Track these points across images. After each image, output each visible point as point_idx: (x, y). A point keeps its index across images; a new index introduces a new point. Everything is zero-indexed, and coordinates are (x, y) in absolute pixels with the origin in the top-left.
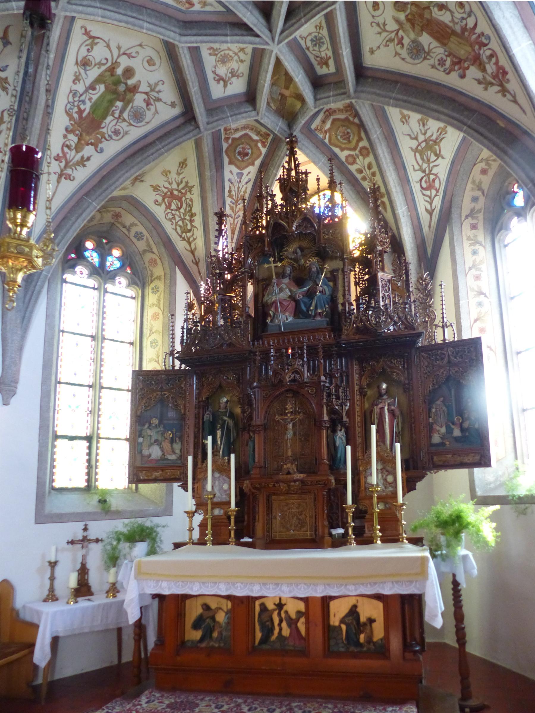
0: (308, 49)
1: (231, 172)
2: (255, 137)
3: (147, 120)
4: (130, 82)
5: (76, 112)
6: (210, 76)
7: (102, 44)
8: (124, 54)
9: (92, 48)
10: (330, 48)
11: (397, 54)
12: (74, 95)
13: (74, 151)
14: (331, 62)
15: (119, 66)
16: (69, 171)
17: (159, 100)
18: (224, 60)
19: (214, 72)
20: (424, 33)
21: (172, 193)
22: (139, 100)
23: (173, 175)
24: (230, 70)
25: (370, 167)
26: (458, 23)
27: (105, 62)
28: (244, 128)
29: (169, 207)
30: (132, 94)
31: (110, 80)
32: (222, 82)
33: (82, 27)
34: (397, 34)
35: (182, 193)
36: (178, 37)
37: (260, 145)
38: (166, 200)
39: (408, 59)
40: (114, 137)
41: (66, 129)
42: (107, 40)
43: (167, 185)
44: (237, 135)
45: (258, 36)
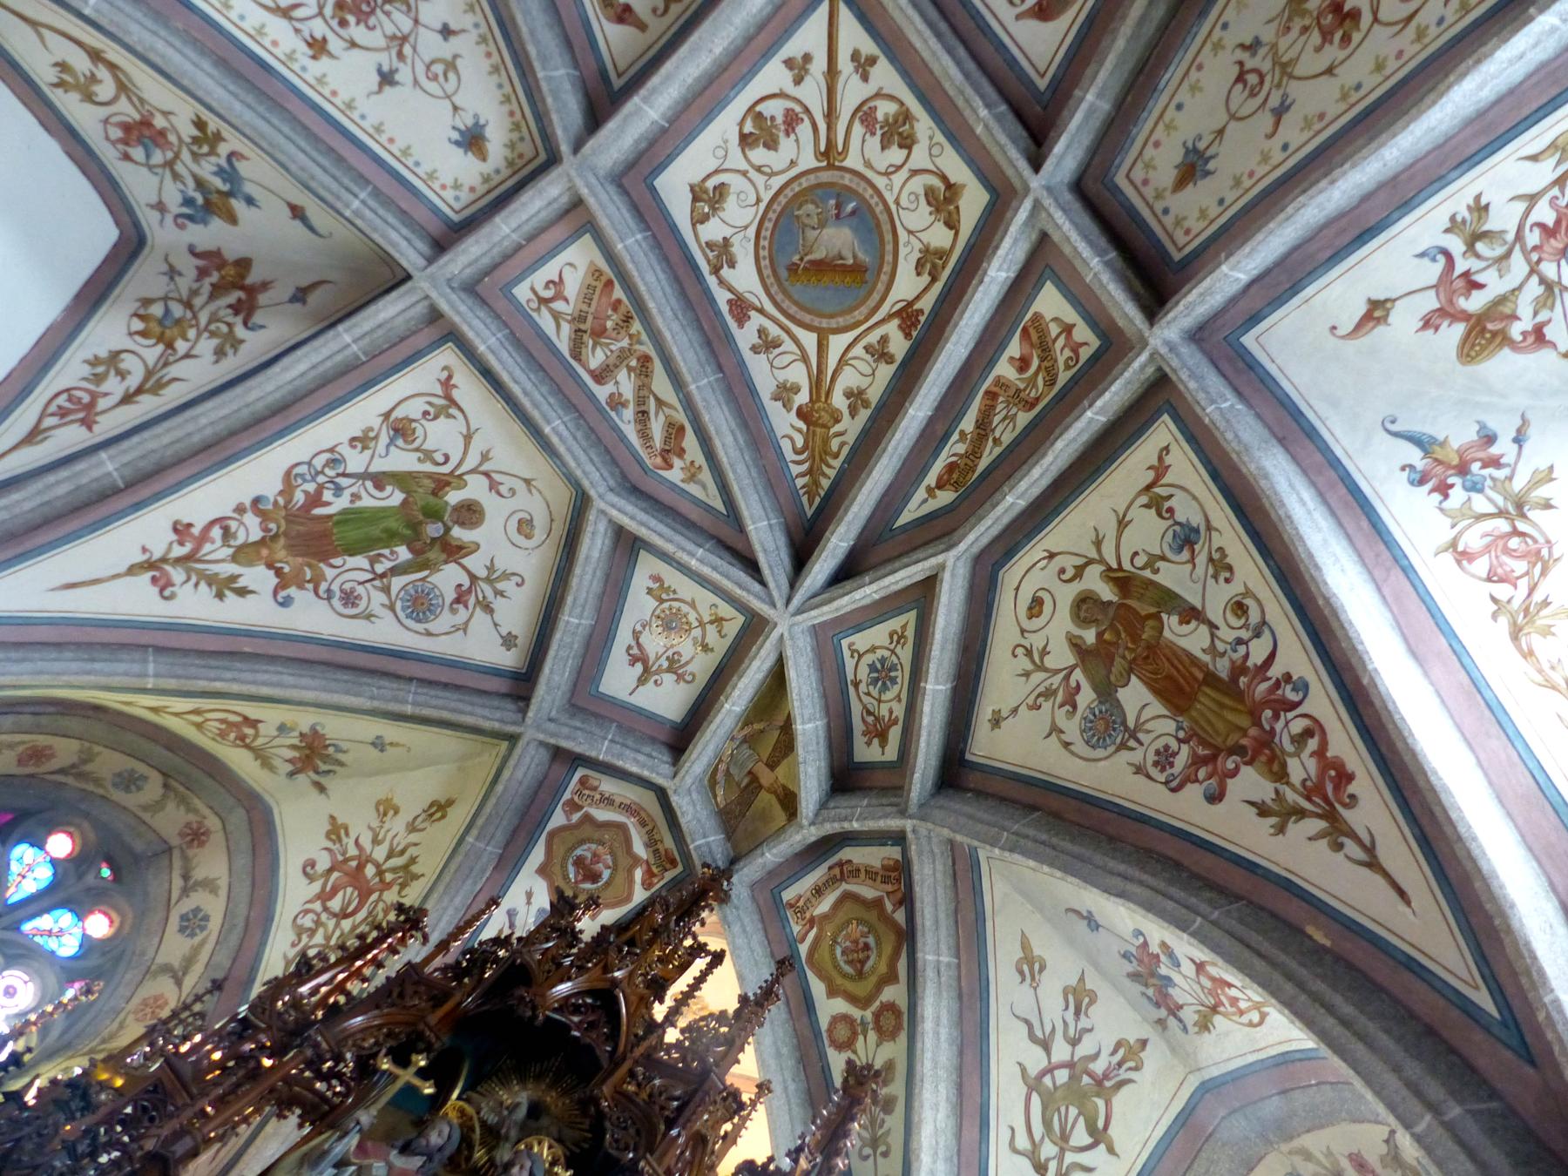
0: (856, 684)
1: (529, 895)
2: (639, 849)
3: (431, 626)
4: (457, 532)
5: (305, 492)
6: (623, 637)
7: (458, 425)
8: (487, 474)
9: (436, 418)
10: (904, 696)
11: (1055, 730)
12: (332, 463)
13: (230, 551)
14: (895, 734)
15: (459, 488)
16: (177, 575)
17: (488, 608)
18: (671, 622)
19: (636, 635)
20: (1133, 678)
21: (360, 868)
22: (448, 578)
23: (397, 825)
24: (670, 653)
26: (1223, 654)
27: (441, 459)
28: (628, 809)
29: (324, 896)
30: (444, 556)
31: (422, 496)
32: (639, 667)
33: (445, 368)
34: (1067, 677)
35: (382, 881)
36: (602, 489)
37: (638, 874)
38: (336, 875)
39: (1080, 747)
40: (336, 602)
41: (256, 501)
42: (473, 428)
43: (366, 841)
44: (602, 815)
45: (763, 583)
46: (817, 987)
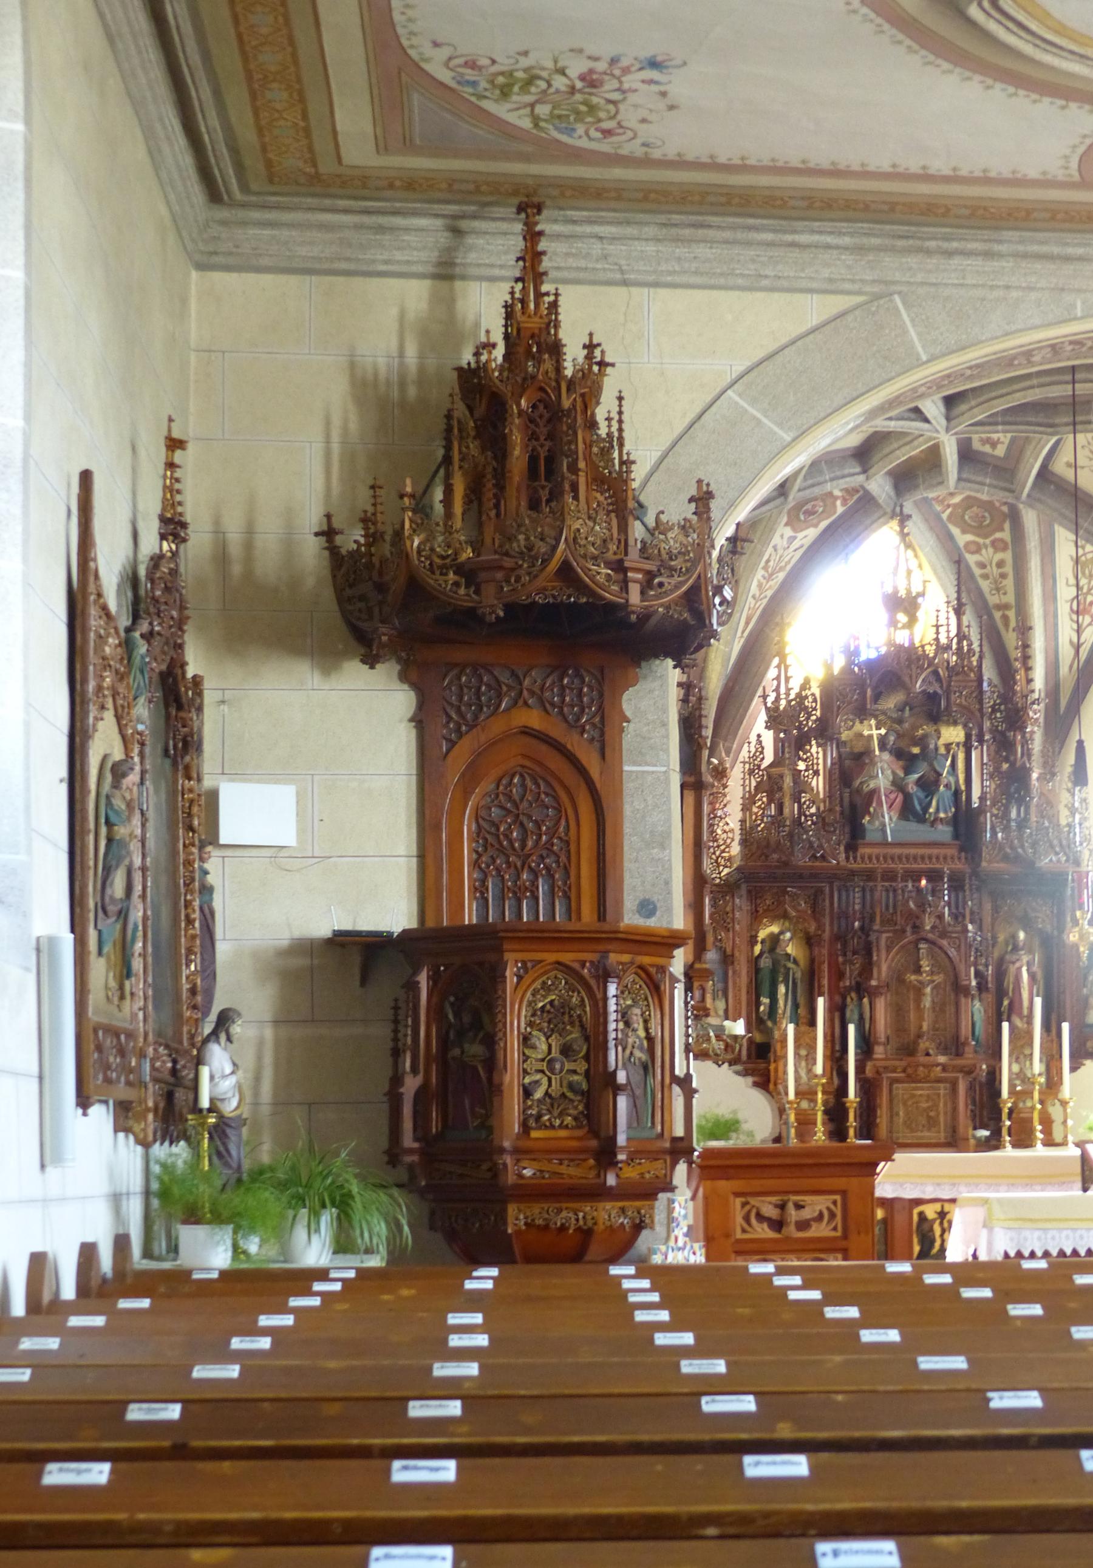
25: (1000, 564)
37: (838, 503)
45: (927, 421)
46: (955, 531)
